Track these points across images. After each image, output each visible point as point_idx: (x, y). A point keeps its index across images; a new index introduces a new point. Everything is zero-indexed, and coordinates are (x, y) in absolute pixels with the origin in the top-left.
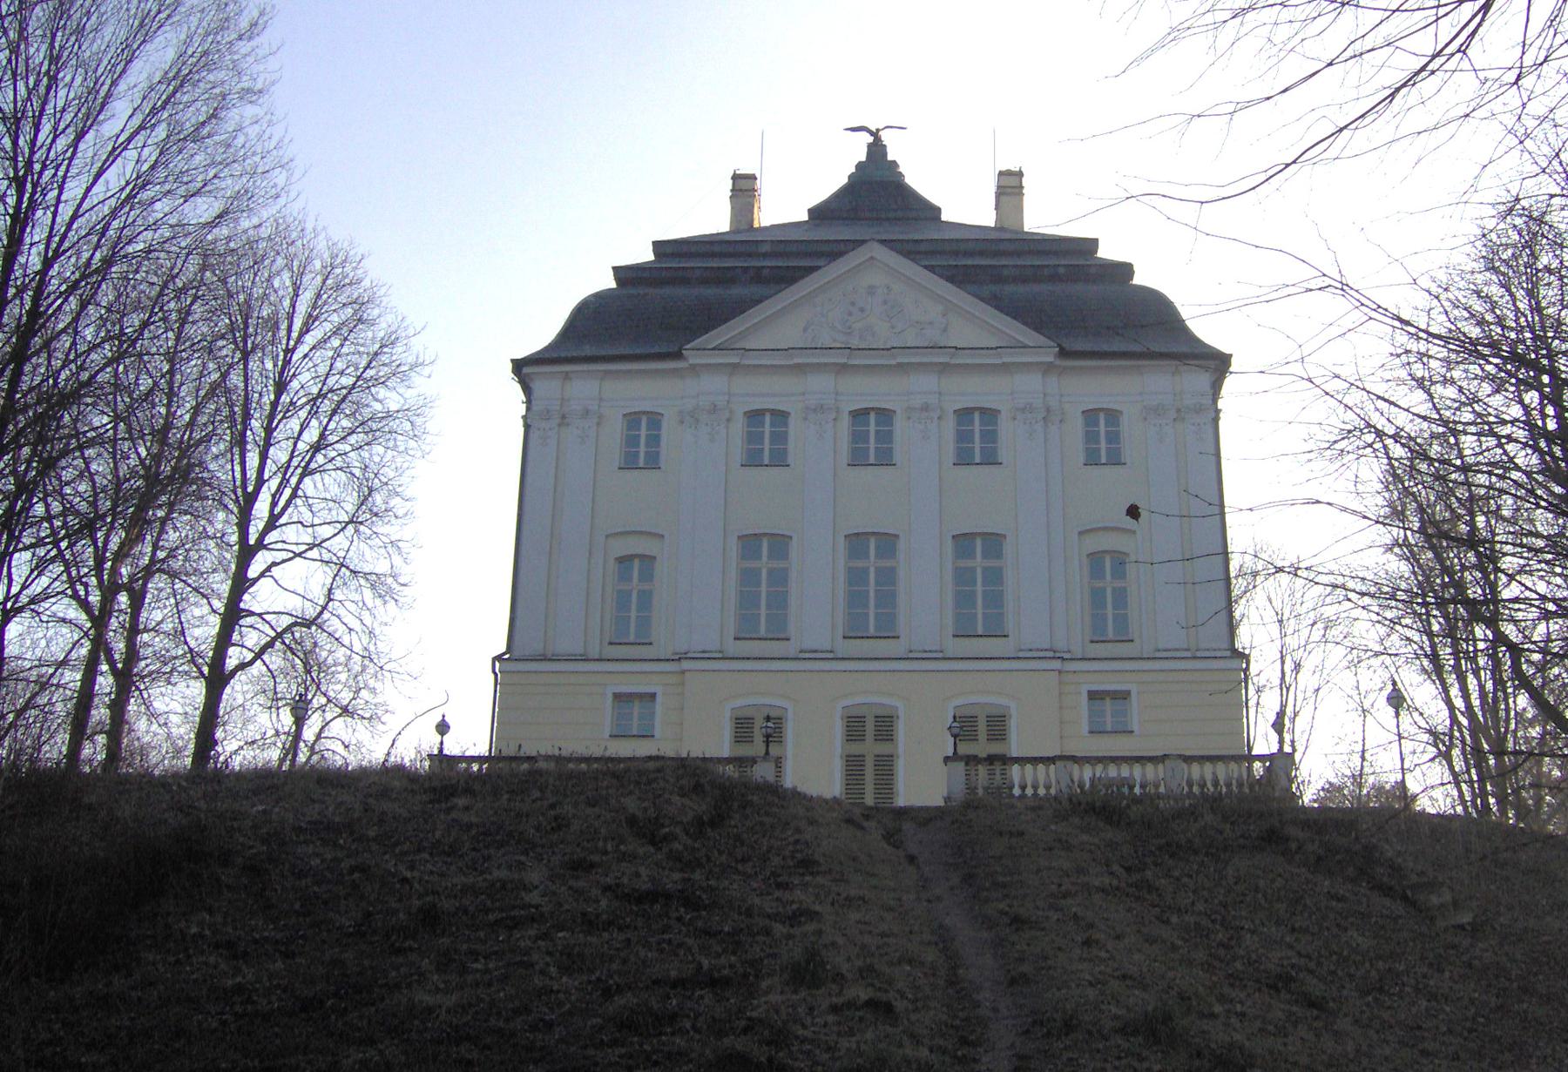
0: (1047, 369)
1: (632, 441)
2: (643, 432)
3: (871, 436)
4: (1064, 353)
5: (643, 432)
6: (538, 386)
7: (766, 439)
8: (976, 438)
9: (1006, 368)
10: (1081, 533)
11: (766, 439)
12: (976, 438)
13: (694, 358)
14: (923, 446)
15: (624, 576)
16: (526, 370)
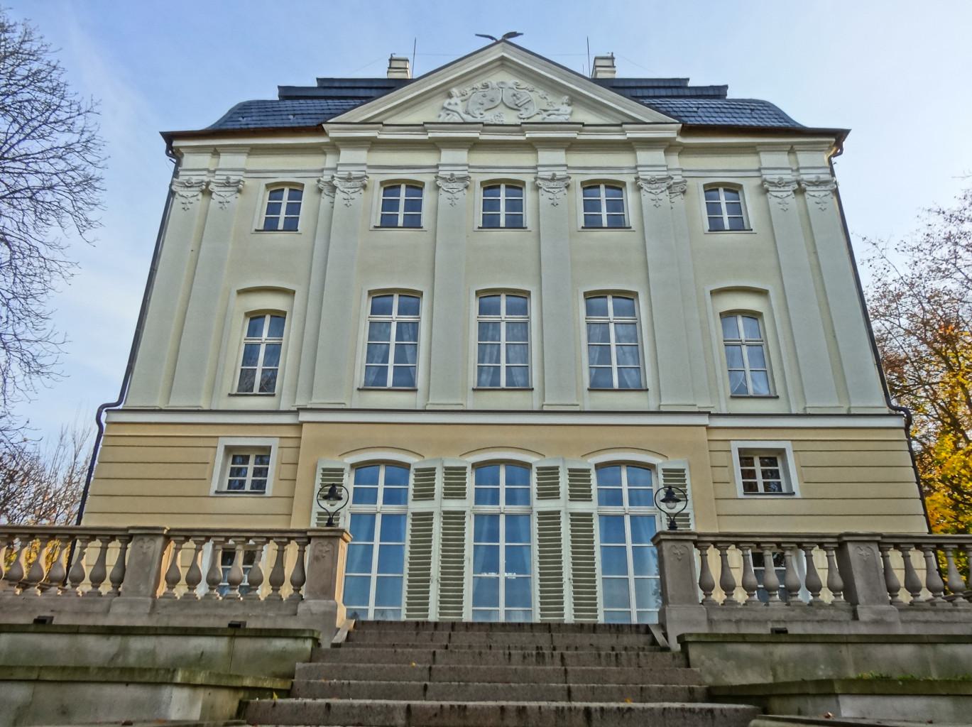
0: (668, 146)
1: (273, 208)
2: (285, 200)
3: (502, 204)
4: (687, 130)
5: (285, 200)
6: (190, 161)
7: (402, 204)
8: (604, 204)
9: (629, 146)
10: (712, 293)
11: (402, 204)
12: (604, 204)
13: (333, 131)
14: (554, 209)
15: (254, 331)
16: (176, 144)
